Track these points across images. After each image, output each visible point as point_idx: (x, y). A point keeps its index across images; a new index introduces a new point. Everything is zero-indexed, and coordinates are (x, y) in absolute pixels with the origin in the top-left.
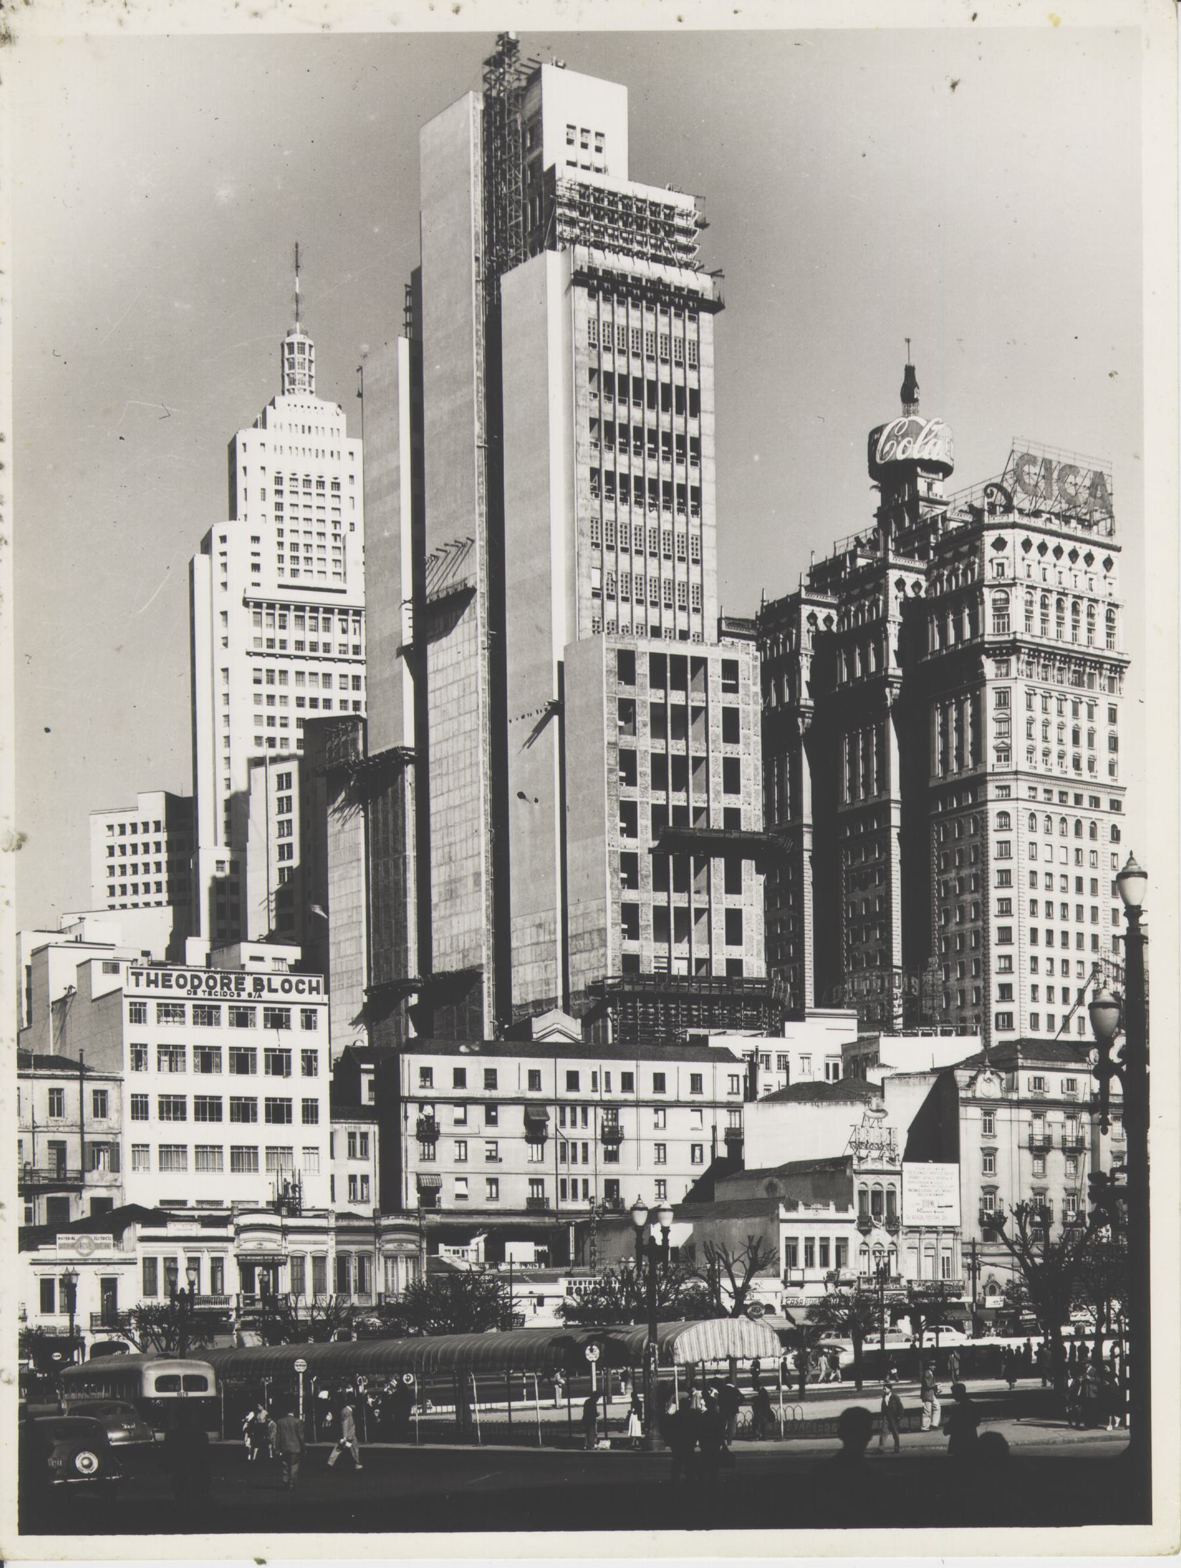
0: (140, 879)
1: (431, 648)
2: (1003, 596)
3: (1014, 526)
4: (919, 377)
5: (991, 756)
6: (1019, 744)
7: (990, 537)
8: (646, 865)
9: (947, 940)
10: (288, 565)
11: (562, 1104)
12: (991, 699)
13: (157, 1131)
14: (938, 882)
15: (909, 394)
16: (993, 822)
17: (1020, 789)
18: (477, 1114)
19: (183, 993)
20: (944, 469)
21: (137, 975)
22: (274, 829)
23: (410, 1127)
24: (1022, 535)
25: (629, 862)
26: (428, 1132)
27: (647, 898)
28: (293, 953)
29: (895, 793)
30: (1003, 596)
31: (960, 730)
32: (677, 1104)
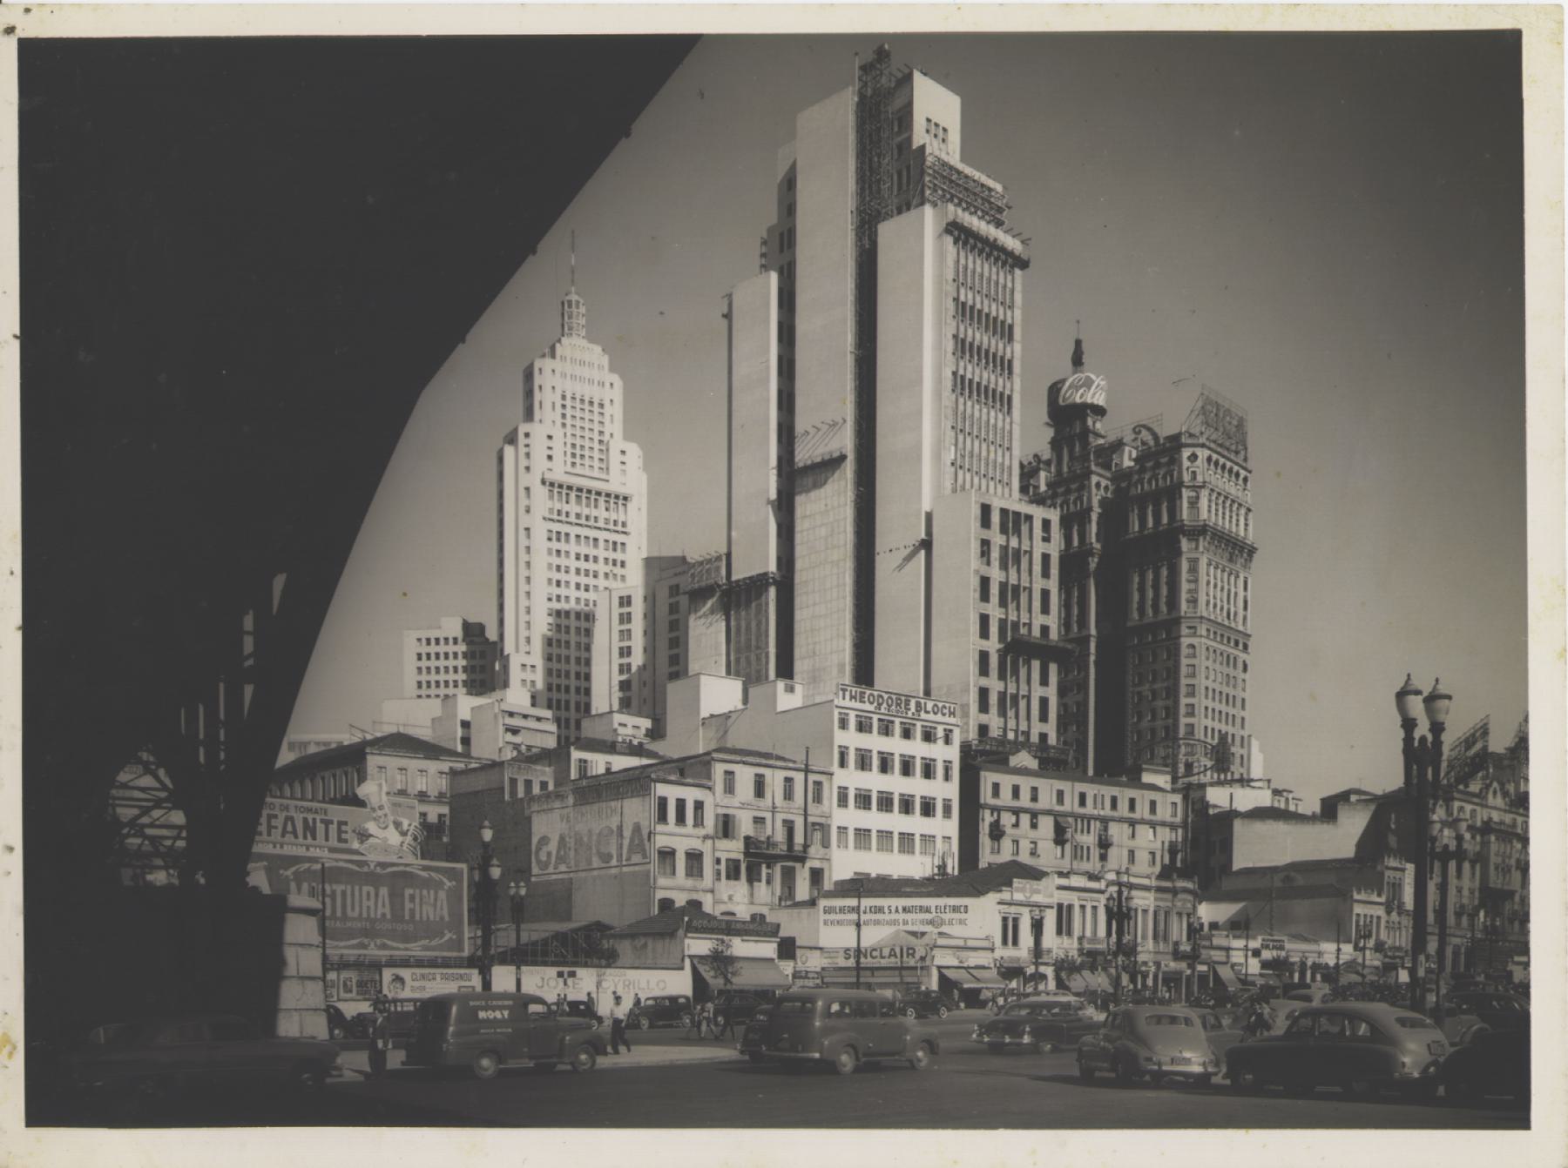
0: (442, 677)
1: (800, 500)
4: (1084, 346)
5: (1184, 606)
6: (1202, 599)
7: (1186, 453)
8: (994, 661)
9: (1139, 733)
10: (569, 459)
11: (1076, 817)
12: (1185, 566)
13: (852, 817)
15: (1077, 361)
16: (1184, 651)
18: (1025, 819)
19: (871, 708)
20: (1099, 411)
21: (844, 690)
22: (616, 636)
23: (985, 828)
24: (1207, 453)
25: (984, 657)
26: (997, 833)
27: (994, 684)
28: (646, 723)
29: (1093, 631)
31: (1156, 587)
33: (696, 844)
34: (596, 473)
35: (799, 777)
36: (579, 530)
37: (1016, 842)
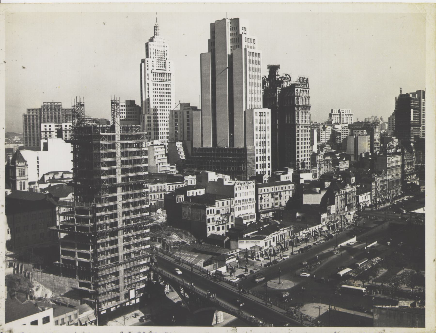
23: (259, 198)
26: (261, 199)
33: (213, 216)
34: (164, 69)
35: (229, 201)
36: (161, 83)
37: (265, 200)
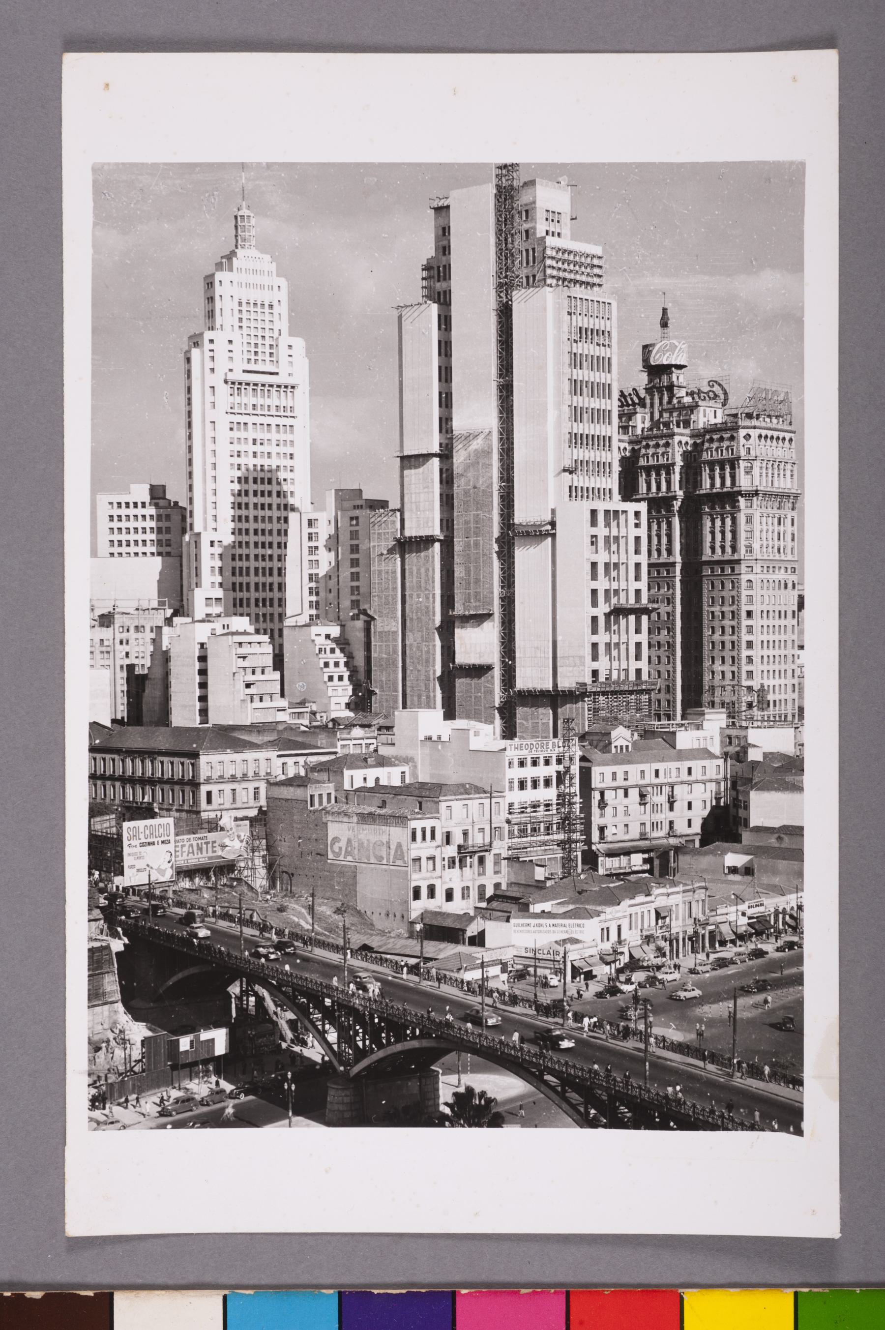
2: (749, 465)
3: (755, 427)
5: (743, 550)
14: (708, 611)
17: (757, 568)
22: (306, 551)
26: (602, 805)
30: (749, 465)
32: (697, 782)
